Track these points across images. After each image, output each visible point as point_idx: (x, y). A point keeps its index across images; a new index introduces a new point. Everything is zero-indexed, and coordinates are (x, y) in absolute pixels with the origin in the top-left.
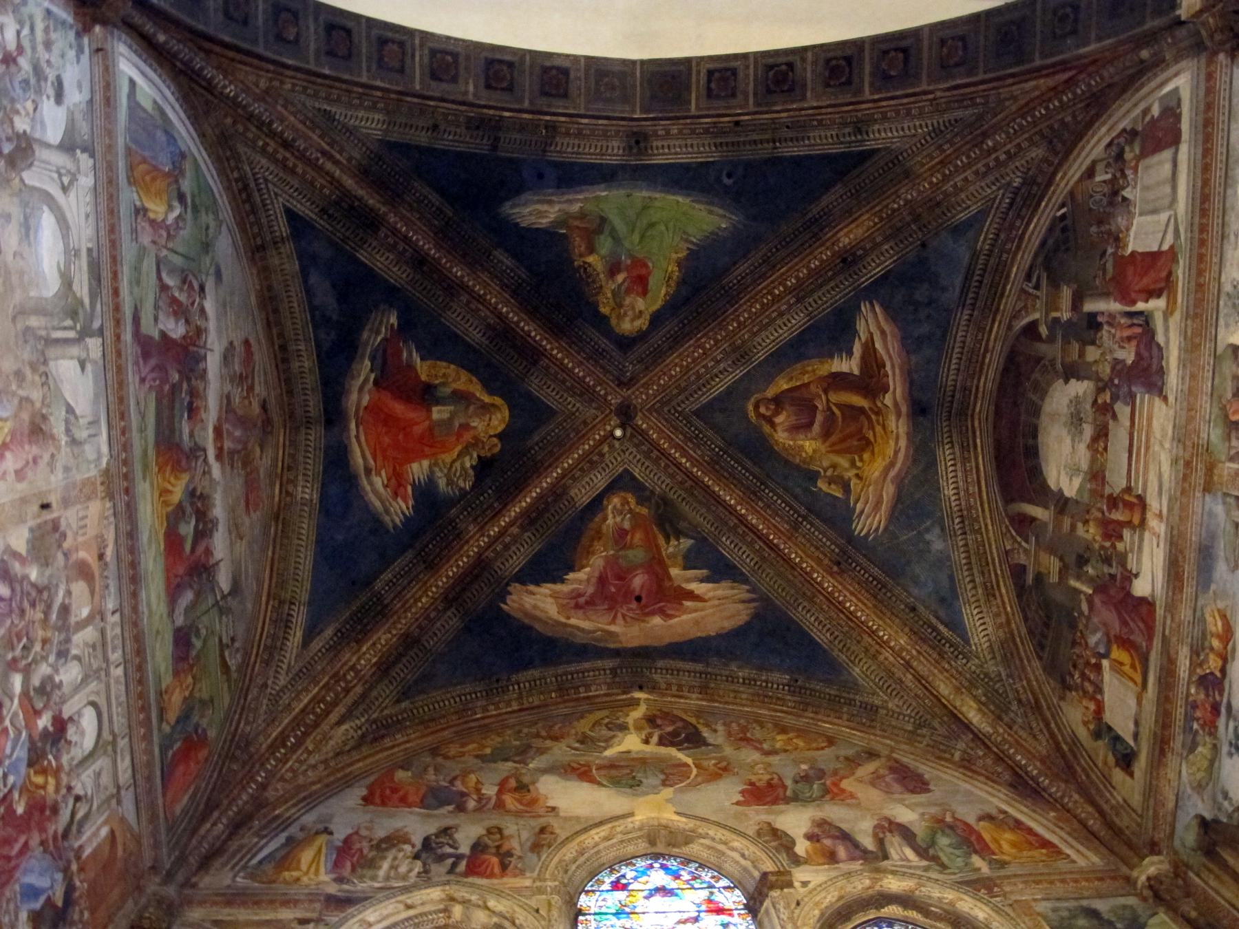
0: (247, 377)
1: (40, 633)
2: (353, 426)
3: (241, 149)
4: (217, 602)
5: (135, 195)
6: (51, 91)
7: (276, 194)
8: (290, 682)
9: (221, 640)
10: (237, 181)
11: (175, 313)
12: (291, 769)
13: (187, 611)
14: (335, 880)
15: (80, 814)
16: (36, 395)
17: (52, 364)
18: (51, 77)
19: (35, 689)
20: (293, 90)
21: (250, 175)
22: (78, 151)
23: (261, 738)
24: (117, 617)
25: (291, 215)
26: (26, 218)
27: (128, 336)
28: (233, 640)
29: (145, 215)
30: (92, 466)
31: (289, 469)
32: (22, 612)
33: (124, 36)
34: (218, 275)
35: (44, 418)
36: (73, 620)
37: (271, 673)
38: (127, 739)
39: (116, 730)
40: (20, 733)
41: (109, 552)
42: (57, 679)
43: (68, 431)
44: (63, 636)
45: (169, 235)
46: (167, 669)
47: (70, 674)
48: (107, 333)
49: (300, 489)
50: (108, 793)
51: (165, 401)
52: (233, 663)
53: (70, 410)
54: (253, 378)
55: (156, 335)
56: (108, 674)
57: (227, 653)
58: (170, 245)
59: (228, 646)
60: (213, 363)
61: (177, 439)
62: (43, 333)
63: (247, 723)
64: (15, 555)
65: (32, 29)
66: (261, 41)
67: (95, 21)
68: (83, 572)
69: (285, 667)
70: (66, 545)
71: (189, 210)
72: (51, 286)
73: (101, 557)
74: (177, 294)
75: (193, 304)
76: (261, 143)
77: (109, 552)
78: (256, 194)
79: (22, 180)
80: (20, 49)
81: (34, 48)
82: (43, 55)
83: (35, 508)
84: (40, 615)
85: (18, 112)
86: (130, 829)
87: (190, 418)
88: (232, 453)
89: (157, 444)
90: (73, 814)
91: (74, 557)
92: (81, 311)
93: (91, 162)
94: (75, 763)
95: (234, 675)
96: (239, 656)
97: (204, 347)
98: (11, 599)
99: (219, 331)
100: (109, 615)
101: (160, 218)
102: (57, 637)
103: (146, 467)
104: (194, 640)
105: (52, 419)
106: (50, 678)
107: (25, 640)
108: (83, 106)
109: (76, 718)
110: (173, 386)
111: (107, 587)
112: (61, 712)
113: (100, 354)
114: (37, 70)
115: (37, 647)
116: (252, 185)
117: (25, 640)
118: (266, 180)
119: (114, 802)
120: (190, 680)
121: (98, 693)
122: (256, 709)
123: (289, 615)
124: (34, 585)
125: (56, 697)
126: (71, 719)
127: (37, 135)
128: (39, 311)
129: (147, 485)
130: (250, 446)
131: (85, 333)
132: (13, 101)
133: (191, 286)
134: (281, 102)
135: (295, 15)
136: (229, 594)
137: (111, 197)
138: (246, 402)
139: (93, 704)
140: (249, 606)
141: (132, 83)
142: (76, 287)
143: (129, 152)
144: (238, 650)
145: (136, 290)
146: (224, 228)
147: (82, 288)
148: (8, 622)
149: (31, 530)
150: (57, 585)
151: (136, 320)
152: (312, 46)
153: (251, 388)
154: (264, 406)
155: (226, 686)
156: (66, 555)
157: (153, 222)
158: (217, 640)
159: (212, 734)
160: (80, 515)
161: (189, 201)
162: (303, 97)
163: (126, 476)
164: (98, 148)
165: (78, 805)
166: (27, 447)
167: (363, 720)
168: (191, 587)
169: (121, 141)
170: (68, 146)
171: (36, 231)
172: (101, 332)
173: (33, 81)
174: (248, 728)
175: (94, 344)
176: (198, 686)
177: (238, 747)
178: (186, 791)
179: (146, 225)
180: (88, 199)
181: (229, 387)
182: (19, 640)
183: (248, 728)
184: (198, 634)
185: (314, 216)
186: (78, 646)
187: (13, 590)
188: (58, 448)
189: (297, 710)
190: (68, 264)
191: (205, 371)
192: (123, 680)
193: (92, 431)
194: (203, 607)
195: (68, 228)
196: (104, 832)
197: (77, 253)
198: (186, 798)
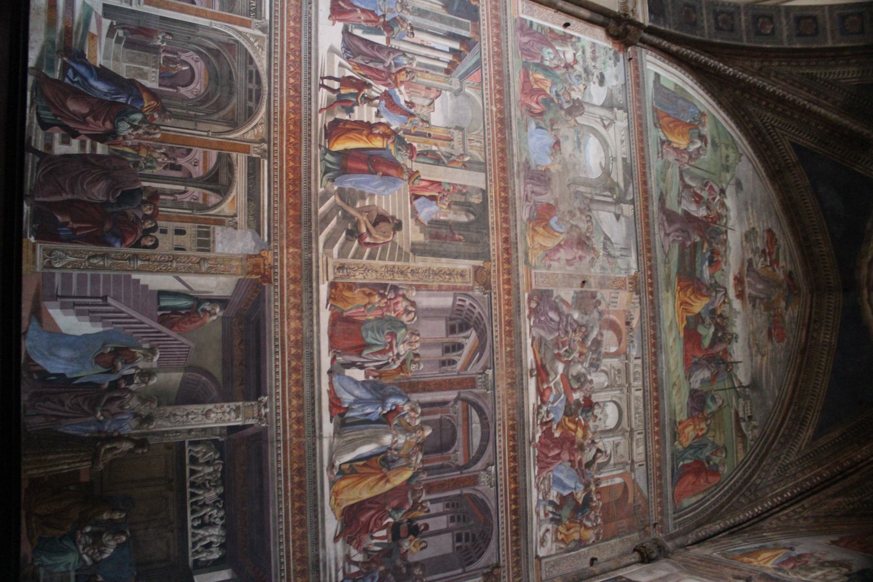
0: (770, 254)
1: (578, 348)
2: (865, 292)
3: (751, 109)
4: (734, 388)
5: (661, 134)
6: (596, 80)
7: (783, 135)
8: (798, 460)
9: (737, 413)
10: (753, 129)
11: (697, 202)
12: (787, 515)
13: (703, 381)
14: (775, 569)
15: (600, 461)
16: (583, 226)
17: (594, 212)
18: (596, 73)
19: (572, 375)
20: (780, 65)
21: (761, 125)
22: (615, 109)
23: (768, 490)
24: (639, 362)
25: (797, 148)
26: (578, 139)
27: (655, 207)
28: (750, 418)
29: (669, 145)
30: (623, 272)
31: (815, 322)
32: (567, 333)
33: (650, 52)
34: (739, 185)
35: (588, 238)
36: (603, 350)
37: (785, 451)
38: (642, 436)
39: (634, 426)
40: (560, 395)
41: (635, 323)
42: (589, 378)
43: (605, 248)
44: (594, 356)
45: (690, 157)
46: (681, 409)
47: (598, 379)
48: (637, 204)
49: (822, 335)
50: (623, 460)
51: (687, 251)
52: (749, 434)
53: (607, 238)
54: (777, 255)
55: (680, 212)
56: (629, 390)
57: (743, 424)
58: (693, 163)
59: (744, 421)
60: (734, 238)
61: (698, 275)
62: (589, 196)
63: (759, 477)
64: (563, 301)
65: (584, 52)
66: (745, 38)
67: (627, 44)
68: (613, 326)
69: (796, 450)
70: (600, 308)
71: (709, 145)
72: (595, 173)
73: (628, 323)
74: (698, 192)
75: (714, 199)
76: (764, 103)
77: (635, 323)
78: (768, 137)
79: (576, 121)
80: (576, 61)
81: (584, 61)
82: (590, 63)
83: (580, 282)
84: (578, 338)
85: (574, 90)
86: (640, 491)
87: (710, 265)
88: (753, 299)
89: (679, 273)
90: (595, 458)
91: (606, 316)
92: (617, 189)
93: (626, 114)
94: (599, 429)
95: (750, 443)
96: (756, 432)
97: (725, 225)
98: (559, 323)
99: (740, 220)
100: (632, 359)
101: (683, 147)
102: (590, 355)
103: (668, 283)
104: (709, 402)
105: (593, 240)
106: (584, 375)
107: (567, 347)
108: (619, 86)
109: (602, 405)
110: (695, 245)
111: (632, 342)
112: (590, 396)
113: (632, 214)
114: (586, 70)
115: (576, 355)
116: (764, 131)
117: (567, 347)
118: (773, 127)
119: (628, 468)
120: (703, 425)
121: (620, 399)
122: (767, 472)
123: (805, 417)
124: (575, 321)
125: (588, 386)
126: (597, 403)
127: (587, 100)
128: (587, 183)
129: (669, 295)
130: (773, 298)
131: (619, 201)
132: (570, 85)
133: (711, 188)
134: (773, 74)
135: (771, 19)
136: (748, 387)
137: (641, 133)
138: (770, 269)
139: (615, 402)
140: (770, 403)
141: (657, 76)
142: (613, 175)
143: (655, 110)
144: (755, 427)
145: (662, 184)
146: (744, 158)
147: (618, 176)
148: (557, 334)
149: (575, 292)
150: (592, 327)
151: (662, 199)
152: (785, 34)
153: (775, 262)
154: (790, 275)
155: (740, 446)
156: (601, 313)
157: (676, 149)
158: (733, 411)
159: (725, 470)
160: (613, 295)
161: (709, 141)
162: (789, 68)
163: (651, 285)
164: (630, 108)
165: (599, 454)
166: (575, 250)
167: (856, 499)
168: (709, 369)
169: (649, 105)
170: (609, 105)
171: (585, 146)
172: (632, 202)
173: (584, 75)
174: (759, 481)
175: (627, 209)
176: (711, 434)
177: (749, 490)
178: (695, 495)
179: (671, 151)
180: (623, 133)
181: (751, 256)
182: (564, 346)
183: (759, 481)
184: (713, 399)
185: (814, 146)
186: (606, 366)
187: (561, 319)
188: (598, 257)
189: (801, 479)
190: (607, 164)
191: (726, 241)
192: (642, 400)
193: (624, 253)
194: (721, 385)
195: (608, 146)
196: (618, 480)
197: (614, 159)
198: (694, 500)
